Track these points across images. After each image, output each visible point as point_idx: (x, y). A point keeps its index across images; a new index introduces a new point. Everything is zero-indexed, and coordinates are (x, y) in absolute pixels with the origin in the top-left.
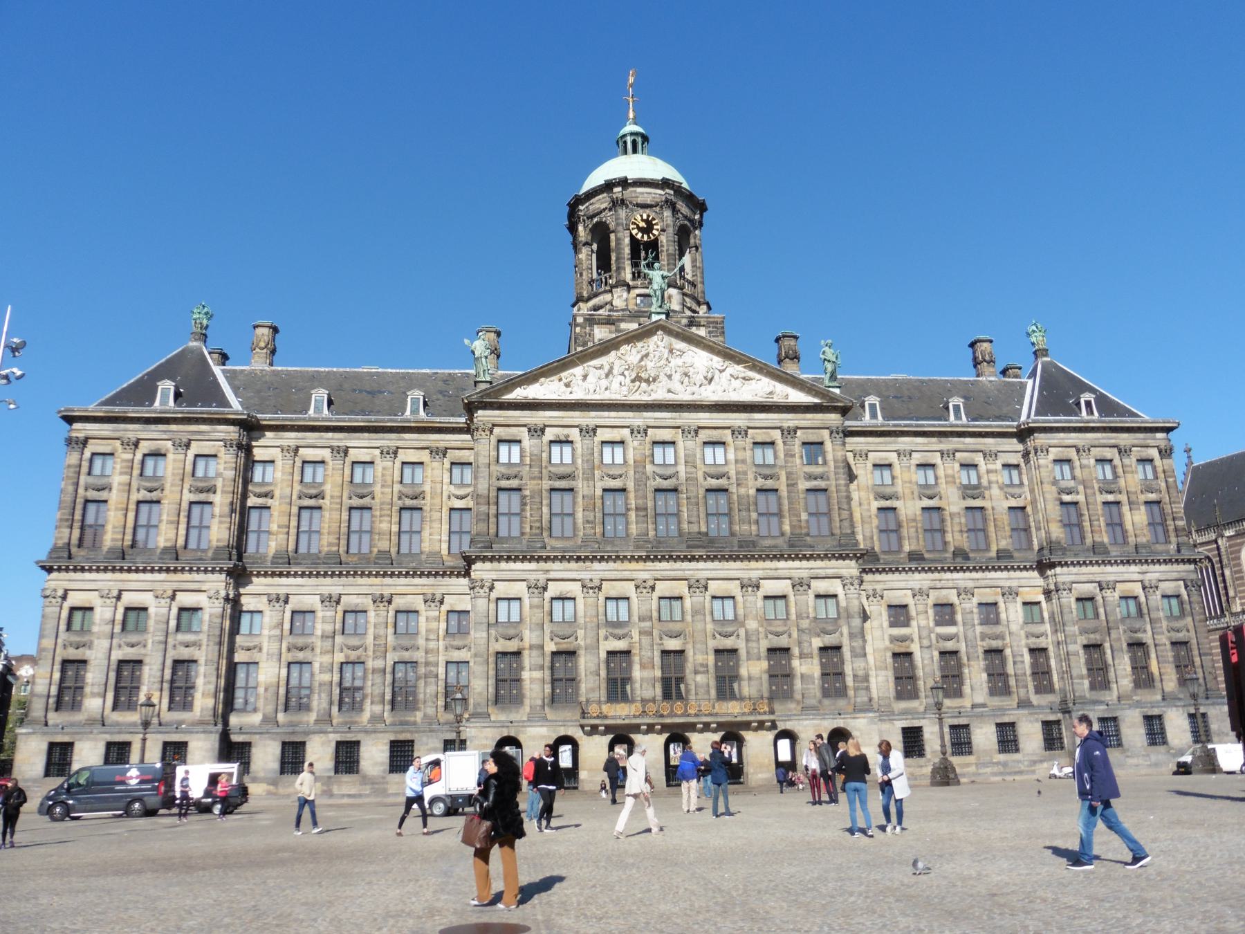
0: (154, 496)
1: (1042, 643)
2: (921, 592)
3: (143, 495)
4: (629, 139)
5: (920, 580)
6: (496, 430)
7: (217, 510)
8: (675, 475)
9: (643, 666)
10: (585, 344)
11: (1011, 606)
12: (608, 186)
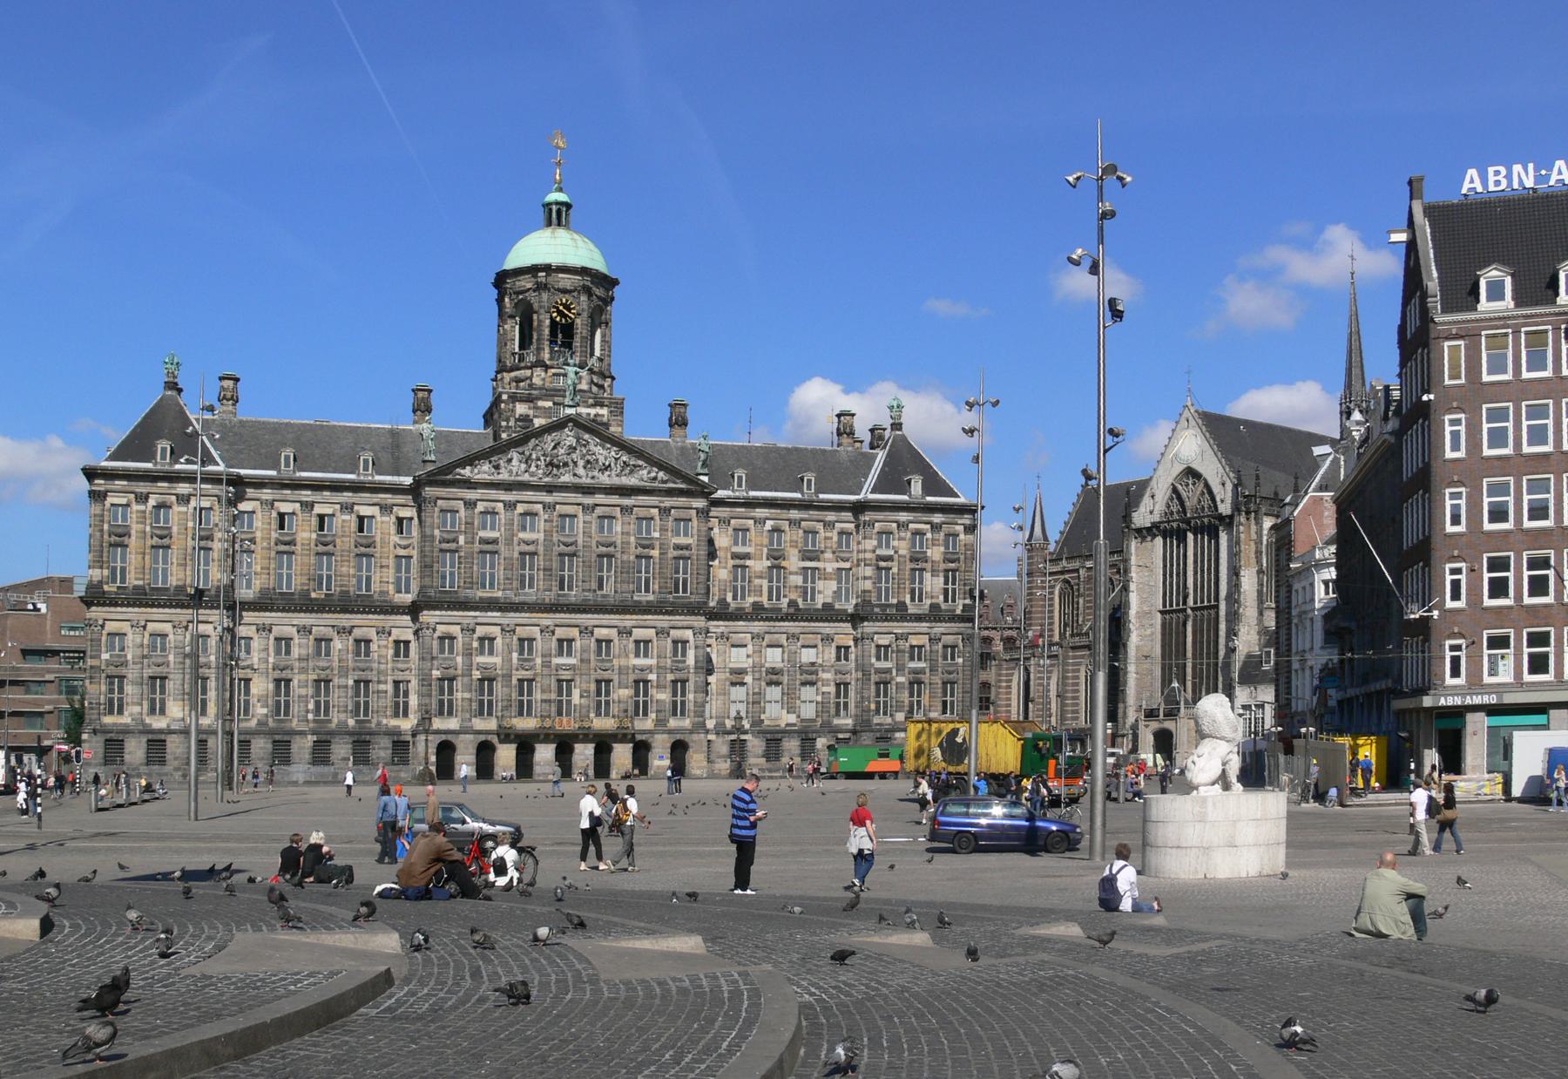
0: (166, 541)
1: (847, 678)
2: (758, 636)
3: (156, 541)
4: (554, 208)
5: (758, 626)
6: (440, 502)
7: (215, 555)
8: (575, 543)
9: (543, 691)
10: (508, 420)
11: (827, 650)
12: (533, 270)
